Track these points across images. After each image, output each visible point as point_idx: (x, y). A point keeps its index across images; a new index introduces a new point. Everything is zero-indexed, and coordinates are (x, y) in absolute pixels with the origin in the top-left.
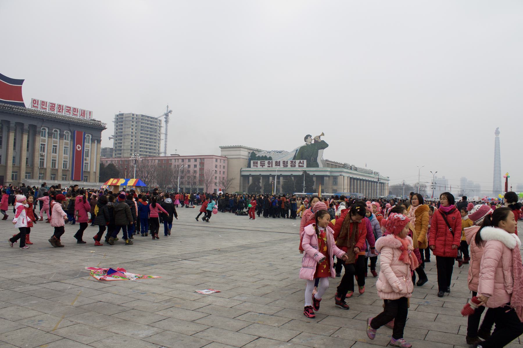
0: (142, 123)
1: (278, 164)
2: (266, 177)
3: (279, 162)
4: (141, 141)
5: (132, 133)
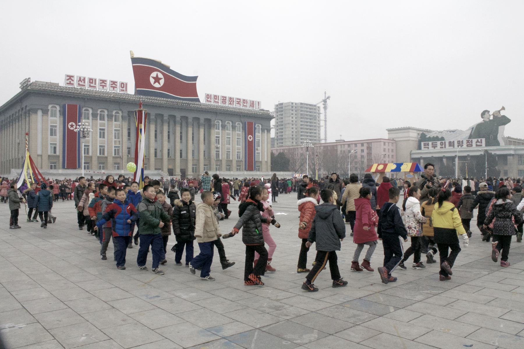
0: (301, 111)
1: (451, 144)
3: (454, 142)
4: (301, 128)
5: (292, 121)
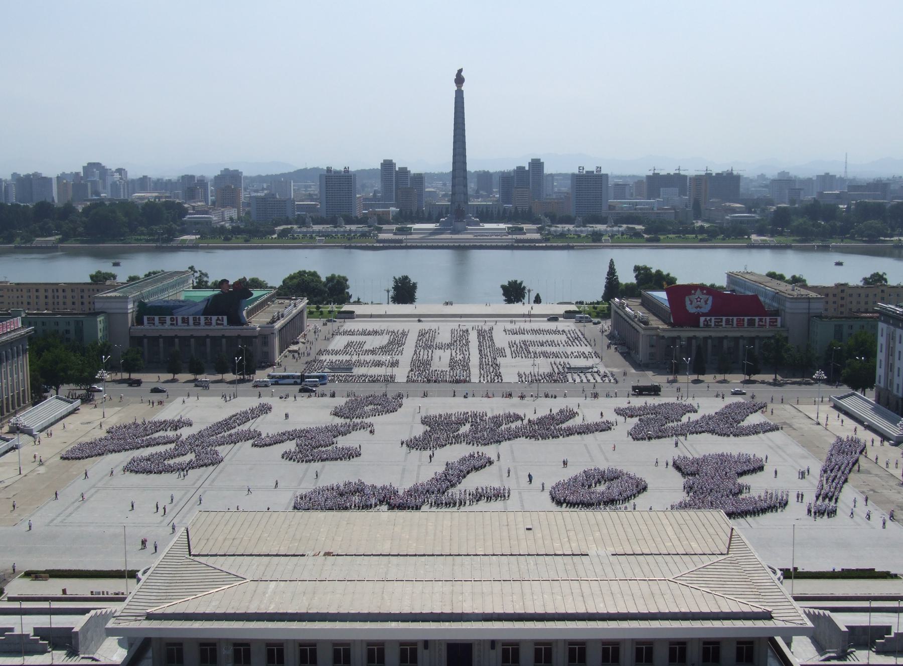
2: (170, 340)
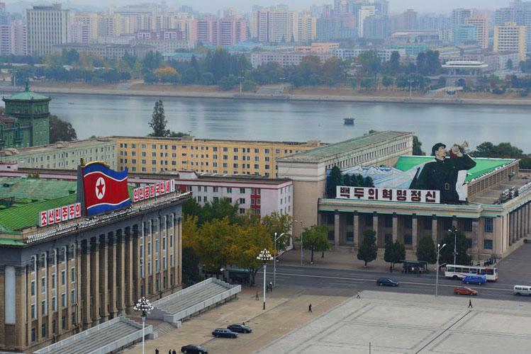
1: (387, 194)
3: (391, 191)
